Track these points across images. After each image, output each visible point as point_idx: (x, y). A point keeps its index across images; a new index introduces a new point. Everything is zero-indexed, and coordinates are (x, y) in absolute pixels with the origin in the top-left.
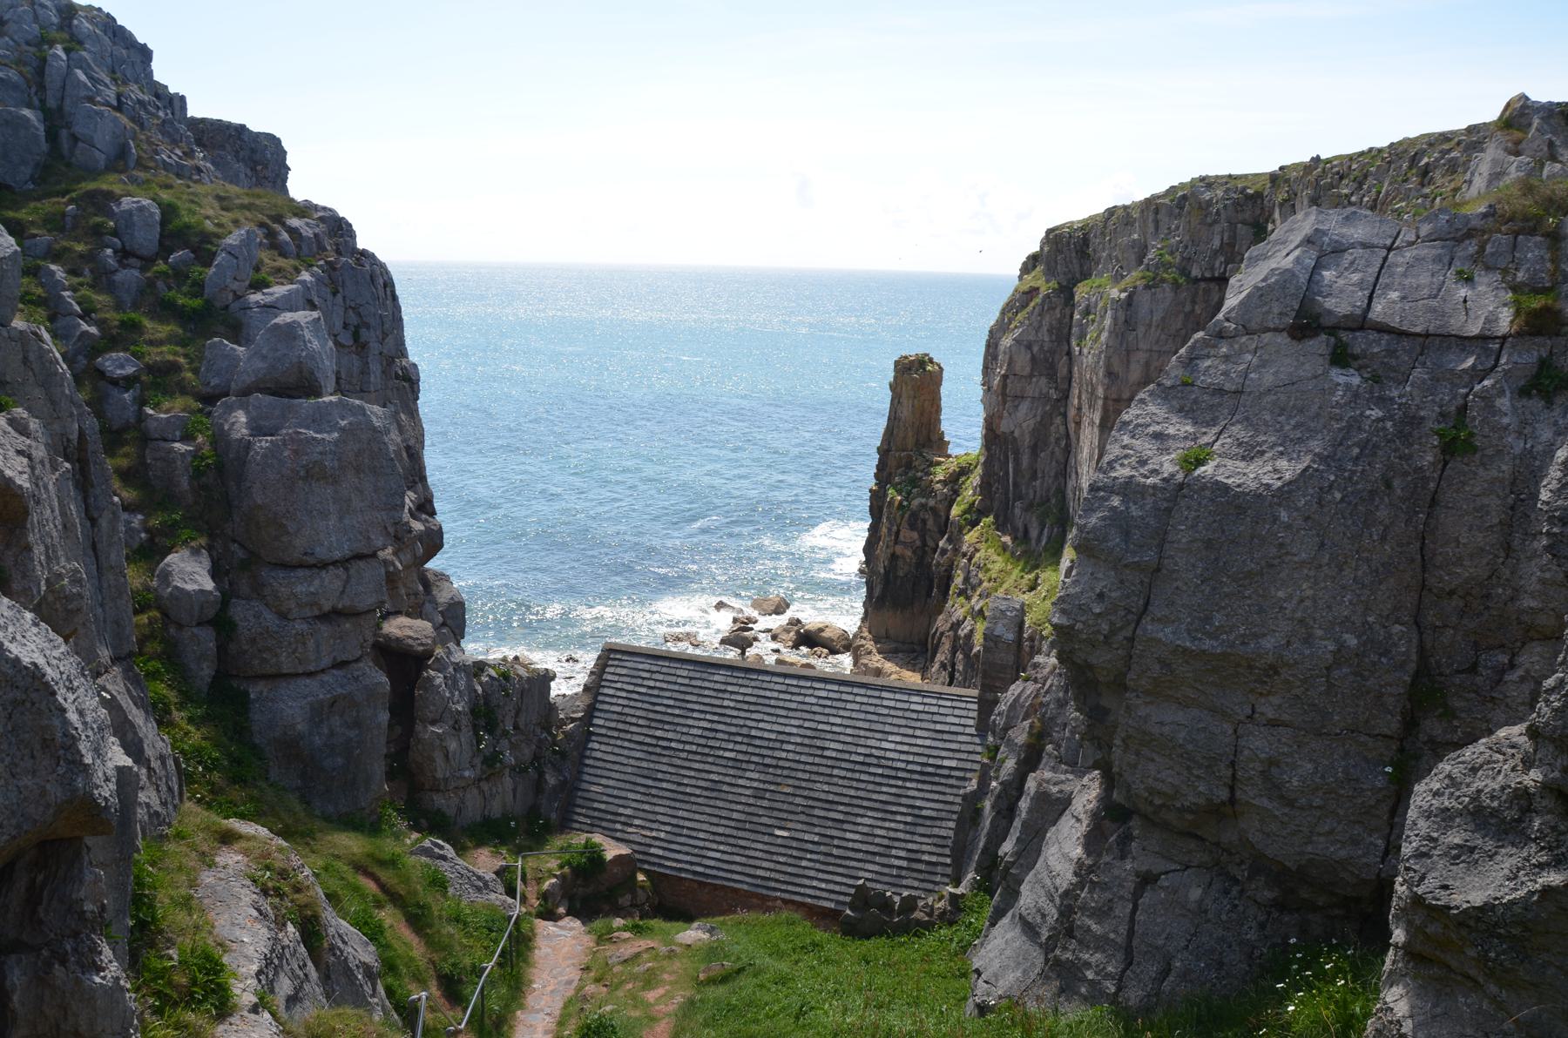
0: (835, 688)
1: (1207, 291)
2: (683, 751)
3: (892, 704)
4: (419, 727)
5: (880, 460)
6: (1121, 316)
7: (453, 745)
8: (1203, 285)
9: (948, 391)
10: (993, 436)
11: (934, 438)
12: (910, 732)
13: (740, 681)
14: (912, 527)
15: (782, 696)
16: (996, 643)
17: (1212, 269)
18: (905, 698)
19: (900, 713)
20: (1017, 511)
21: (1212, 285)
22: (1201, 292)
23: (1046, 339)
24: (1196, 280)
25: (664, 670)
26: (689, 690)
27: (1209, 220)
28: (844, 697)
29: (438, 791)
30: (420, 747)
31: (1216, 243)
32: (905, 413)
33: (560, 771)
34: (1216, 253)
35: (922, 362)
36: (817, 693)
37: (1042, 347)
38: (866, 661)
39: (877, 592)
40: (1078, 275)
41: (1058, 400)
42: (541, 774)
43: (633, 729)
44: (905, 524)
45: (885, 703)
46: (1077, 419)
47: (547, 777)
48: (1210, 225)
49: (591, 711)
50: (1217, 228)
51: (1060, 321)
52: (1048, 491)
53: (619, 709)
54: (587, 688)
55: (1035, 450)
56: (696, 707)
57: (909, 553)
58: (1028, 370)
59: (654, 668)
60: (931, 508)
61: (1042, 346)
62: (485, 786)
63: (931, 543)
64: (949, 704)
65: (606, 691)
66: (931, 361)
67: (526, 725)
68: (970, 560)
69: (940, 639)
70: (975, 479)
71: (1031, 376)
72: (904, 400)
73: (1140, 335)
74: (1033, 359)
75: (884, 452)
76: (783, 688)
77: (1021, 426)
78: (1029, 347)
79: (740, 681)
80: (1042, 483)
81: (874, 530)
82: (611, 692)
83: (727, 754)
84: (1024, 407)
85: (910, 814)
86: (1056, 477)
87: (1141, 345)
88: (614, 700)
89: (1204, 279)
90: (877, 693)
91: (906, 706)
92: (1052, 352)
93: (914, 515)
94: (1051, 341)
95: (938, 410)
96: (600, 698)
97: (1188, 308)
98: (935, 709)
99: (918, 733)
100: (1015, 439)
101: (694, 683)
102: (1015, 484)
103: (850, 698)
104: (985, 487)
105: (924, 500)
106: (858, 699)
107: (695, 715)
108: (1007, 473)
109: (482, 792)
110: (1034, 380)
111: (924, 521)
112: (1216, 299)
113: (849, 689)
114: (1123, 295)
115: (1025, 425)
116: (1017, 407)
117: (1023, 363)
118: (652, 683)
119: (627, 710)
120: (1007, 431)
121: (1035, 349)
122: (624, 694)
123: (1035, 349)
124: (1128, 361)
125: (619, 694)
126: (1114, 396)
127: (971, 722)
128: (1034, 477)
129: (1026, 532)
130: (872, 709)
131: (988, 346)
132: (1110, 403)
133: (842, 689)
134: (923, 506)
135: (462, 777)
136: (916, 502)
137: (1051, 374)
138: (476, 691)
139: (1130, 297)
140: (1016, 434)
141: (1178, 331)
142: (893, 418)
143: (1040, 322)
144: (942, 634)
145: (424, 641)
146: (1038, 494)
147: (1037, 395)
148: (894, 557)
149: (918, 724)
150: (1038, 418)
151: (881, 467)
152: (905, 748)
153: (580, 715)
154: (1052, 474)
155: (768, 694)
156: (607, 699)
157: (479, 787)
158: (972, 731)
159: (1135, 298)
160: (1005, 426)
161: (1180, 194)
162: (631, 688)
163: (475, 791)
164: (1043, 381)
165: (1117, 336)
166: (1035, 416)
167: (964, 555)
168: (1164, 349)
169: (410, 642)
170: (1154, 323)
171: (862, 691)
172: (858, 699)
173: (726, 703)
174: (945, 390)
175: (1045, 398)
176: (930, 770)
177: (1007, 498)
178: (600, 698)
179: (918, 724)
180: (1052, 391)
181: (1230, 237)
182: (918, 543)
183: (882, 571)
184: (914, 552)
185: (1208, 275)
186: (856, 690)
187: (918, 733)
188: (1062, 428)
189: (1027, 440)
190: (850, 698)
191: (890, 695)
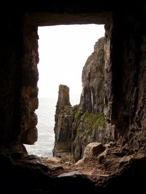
9: (71, 93)
10: (87, 91)
14: (65, 122)
20: (95, 107)
32: (62, 97)
37: (98, 65)
38: (56, 155)
39: (58, 138)
44: (64, 121)
55: (99, 90)
57: (65, 128)
58: (95, 70)
63: (70, 125)
68: (83, 122)
69: (76, 145)
71: (96, 71)
72: (62, 94)
74: (96, 68)
75: (57, 106)
78: (95, 65)
81: (56, 125)
84: (95, 79)
93: (66, 118)
95: (69, 98)
100: (93, 88)
102: (94, 101)
110: (97, 73)
111: (68, 120)
116: (93, 80)
117: (94, 68)
121: (97, 65)
128: (99, 97)
129: (98, 111)
131: (83, 71)
134: (68, 116)
136: (66, 116)
142: (59, 98)
143: (98, 59)
144: (76, 144)
146: (101, 101)
148: (61, 129)
151: (57, 110)
164: (99, 73)
167: (81, 121)
174: (70, 93)
177: (91, 105)
182: (67, 125)
183: (59, 133)
184: (66, 128)
189: (96, 88)
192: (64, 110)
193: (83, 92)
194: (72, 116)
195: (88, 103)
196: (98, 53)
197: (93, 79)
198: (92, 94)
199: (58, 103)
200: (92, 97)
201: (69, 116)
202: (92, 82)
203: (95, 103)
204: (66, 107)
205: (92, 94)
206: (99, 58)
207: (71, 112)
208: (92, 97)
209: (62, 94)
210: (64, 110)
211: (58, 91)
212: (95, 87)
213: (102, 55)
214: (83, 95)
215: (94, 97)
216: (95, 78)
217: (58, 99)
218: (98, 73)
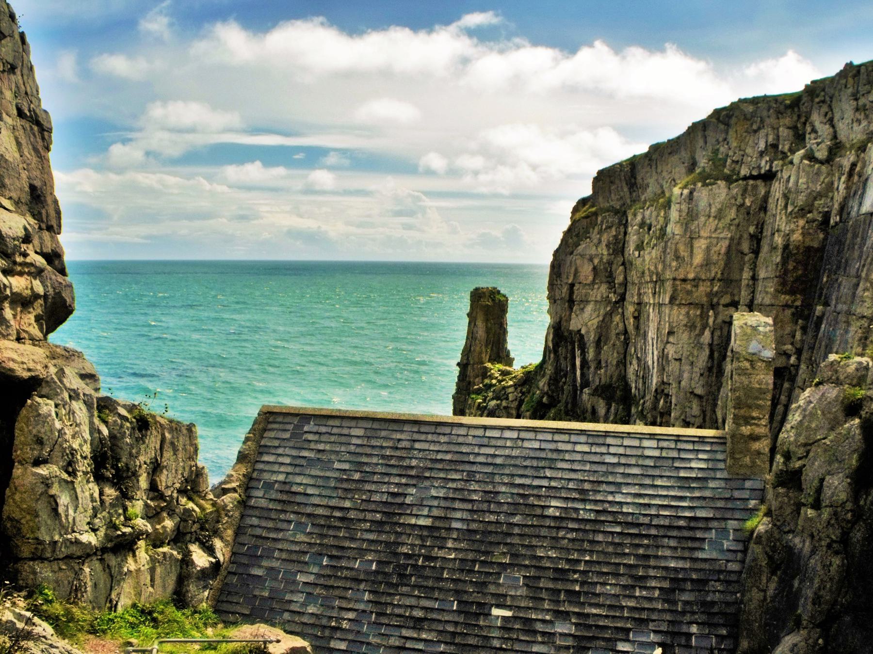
0: (549, 437)
1: (755, 187)
2: (365, 521)
3: (621, 451)
4: (17, 471)
5: (460, 372)
6: (684, 207)
7: (64, 499)
8: (751, 182)
11: (503, 354)
12: (648, 481)
13: (430, 437)
15: (484, 450)
16: (752, 362)
17: (759, 167)
18: (636, 443)
19: (633, 461)
20: (585, 397)
21: (759, 182)
22: (749, 188)
23: (605, 253)
24: (745, 178)
25: (335, 431)
26: (369, 451)
27: (755, 127)
28: (561, 446)
29: (42, 559)
30: (17, 497)
31: (762, 145)
33: (210, 550)
34: (762, 154)
35: (494, 293)
36: (526, 444)
40: (628, 201)
41: (616, 302)
42: (187, 554)
43: (299, 499)
45: (612, 450)
46: (636, 314)
47: (195, 557)
48: (755, 131)
49: (248, 484)
50: (762, 133)
51: (616, 237)
52: (611, 377)
53: (281, 478)
54: (242, 457)
55: (598, 344)
56: (379, 469)
58: (591, 278)
59: (323, 429)
60: (505, 408)
61: (601, 259)
62: (112, 560)
64: (690, 447)
65: (266, 458)
66: (499, 292)
67: (167, 487)
70: (543, 383)
71: (594, 280)
73: (701, 225)
74: (595, 269)
76: (485, 441)
77: (586, 325)
79: (430, 437)
80: (606, 371)
82: (271, 459)
83: (422, 522)
84: (589, 308)
85: (665, 578)
86: (617, 365)
87: (702, 233)
88: (276, 468)
89: (752, 177)
90: (601, 441)
91: (639, 452)
92: (610, 263)
94: (609, 254)
95: (505, 332)
96: (260, 466)
97: (739, 200)
98: (675, 454)
99: (659, 482)
100: (582, 336)
101: (374, 442)
102: (582, 374)
103: (569, 447)
104: (554, 381)
105: (499, 402)
106: (579, 448)
107: (376, 478)
108: (574, 365)
109: (107, 568)
110: (596, 286)
112: (763, 192)
113: (565, 438)
114: (686, 192)
115: (590, 323)
116: (583, 309)
118: (321, 447)
119: (291, 478)
120: (576, 329)
121: (596, 261)
122: (287, 460)
123: (596, 261)
124: (692, 247)
125: (281, 460)
126: (682, 277)
127: (721, 465)
128: (599, 366)
130: (596, 459)
132: (678, 283)
133: (557, 437)
134: (498, 406)
135: (77, 542)
137: (610, 279)
138: (99, 432)
139: (691, 193)
140: (583, 332)
141: (731, 220)
142: (471, 336)
145: (31, 365)
147: (599, 298)
149: (657, 472)
150: (601, 318)
152: (646, 501)
153: (234, 485)
154: (615, 363)
155: (464, 449)
156: (267, 468)
157: (102, 560)
158: (725, 475)
159: (695, 194)
160: (574, 325)
161: (724, 113)
162: (294, 453)
163: (97, 565)
164: (604, 288)
165: (682, 225)
166: (598, 316)
168: (722, 236)
169: (11, 365)
170: (713, 214)
171: (583, 439)
172: (579, 448)
173: (414, 463)
175: (607, 300)
176: (682, 523)
177: (575, 386)
178: (260, 466)
179: (657, 472)
180: (611, 295)
181: (774, 139)
185: (755, 173)
186: (574, 438)
187: (659, 482)
188: (621, 325)
189: (591, 338)
190: (569, 447)
191: (618, 442)
192: (487, 381)
193: (551, 337)
194: (516, 404)
195: (565, 376)
196: (602, 222)
197: (582, 306)
198: (578, 353)
199: (467, 352)
200: (578, 362)
201: (504, 403)
202: (580, 317)
203: (585, 384)
204: (495, 369)
205: (578, 353)
206: (605, 238)
207: (511, 390)
208: (578, 362)
209: (480, 324)
210: (487, 381)
211: (468, 310)
212: (588, 332)
213: (614, 229)
214: (551, 345)
215: (584, 364)
216: (588, 302)
217: (467, 338)
218: (599, 288)
